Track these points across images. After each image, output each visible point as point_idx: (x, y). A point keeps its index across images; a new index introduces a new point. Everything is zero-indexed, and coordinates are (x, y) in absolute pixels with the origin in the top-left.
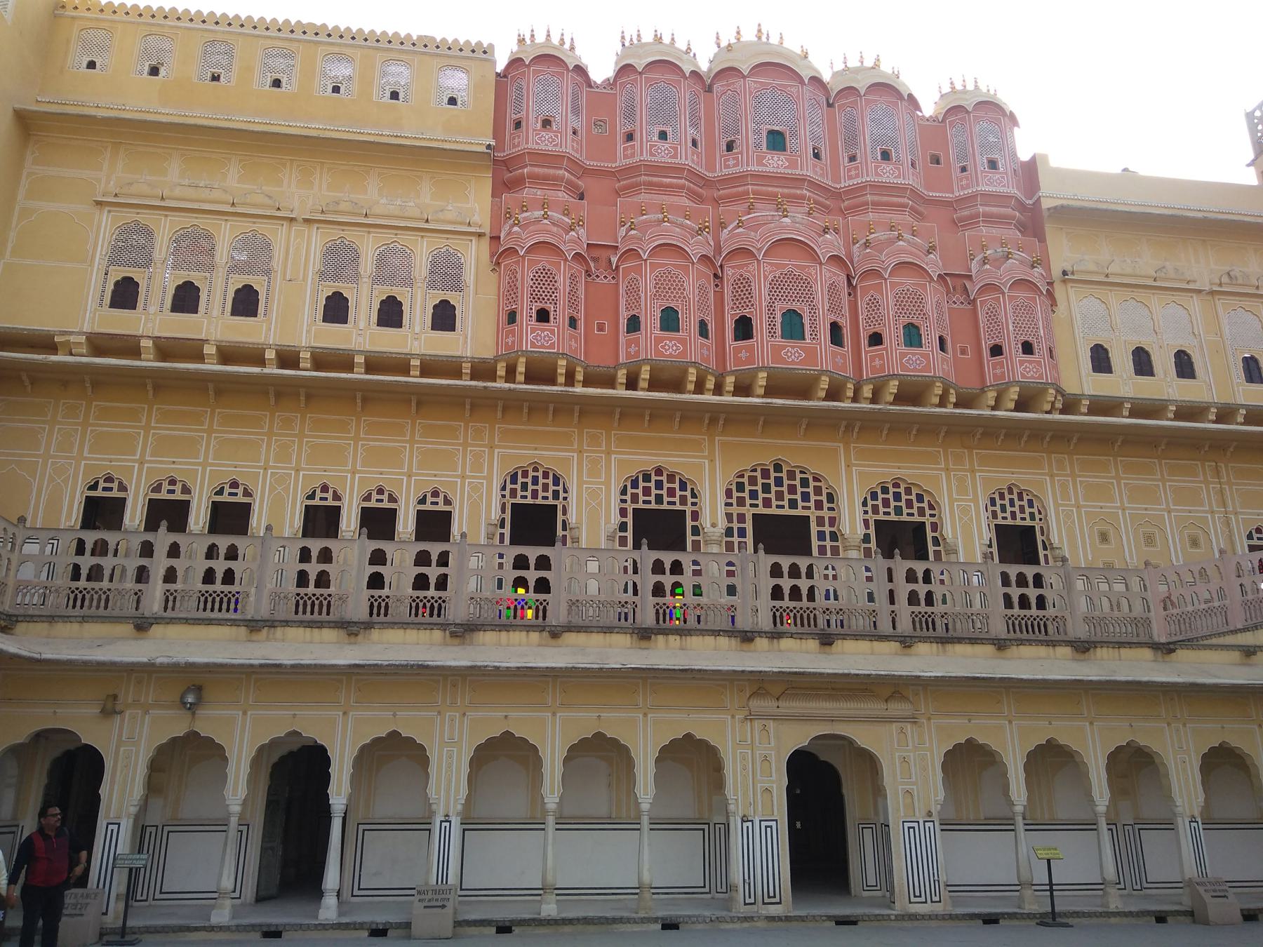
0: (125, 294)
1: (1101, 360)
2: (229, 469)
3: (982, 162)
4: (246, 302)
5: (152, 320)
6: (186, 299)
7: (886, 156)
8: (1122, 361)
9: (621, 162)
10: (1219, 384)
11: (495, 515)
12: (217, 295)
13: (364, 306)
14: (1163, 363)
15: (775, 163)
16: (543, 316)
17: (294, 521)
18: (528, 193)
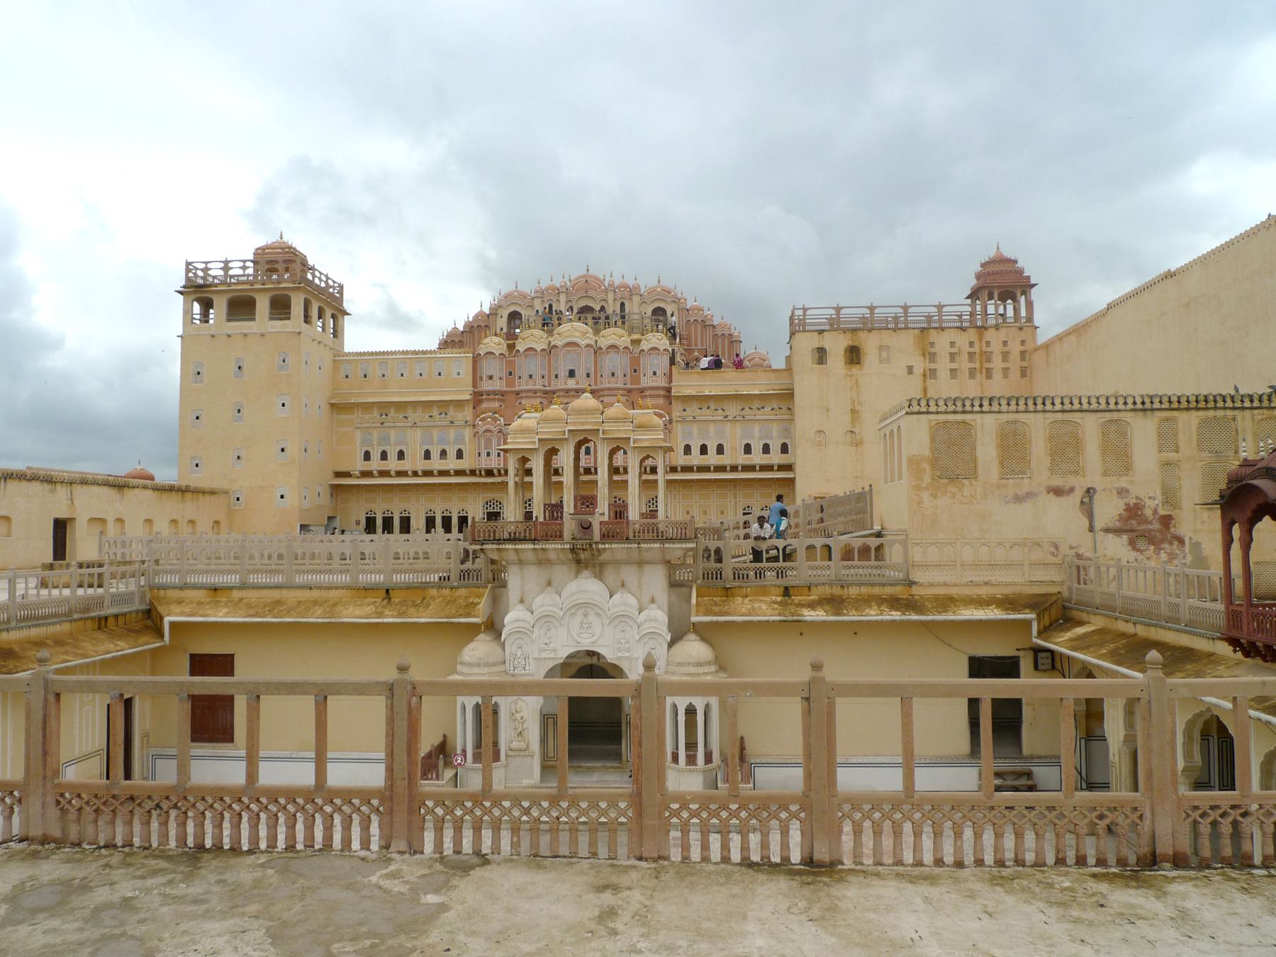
0: (367, 456)
1: (688, 449)
2: (402, 506)
3: (650, 373)
4: (401, 455)
5: (375, 464)
6: (384, 456)
7: (613, 374)
8: (696, 450)
9: (517, 388)
10: (733, 456)
11: (481, 515)
12: (392, 455)
13: (435, 454)
14: (712, 449)
15: (571, 384)
16: (488, 454)
17: (423, 522)
18: (485, 405)
